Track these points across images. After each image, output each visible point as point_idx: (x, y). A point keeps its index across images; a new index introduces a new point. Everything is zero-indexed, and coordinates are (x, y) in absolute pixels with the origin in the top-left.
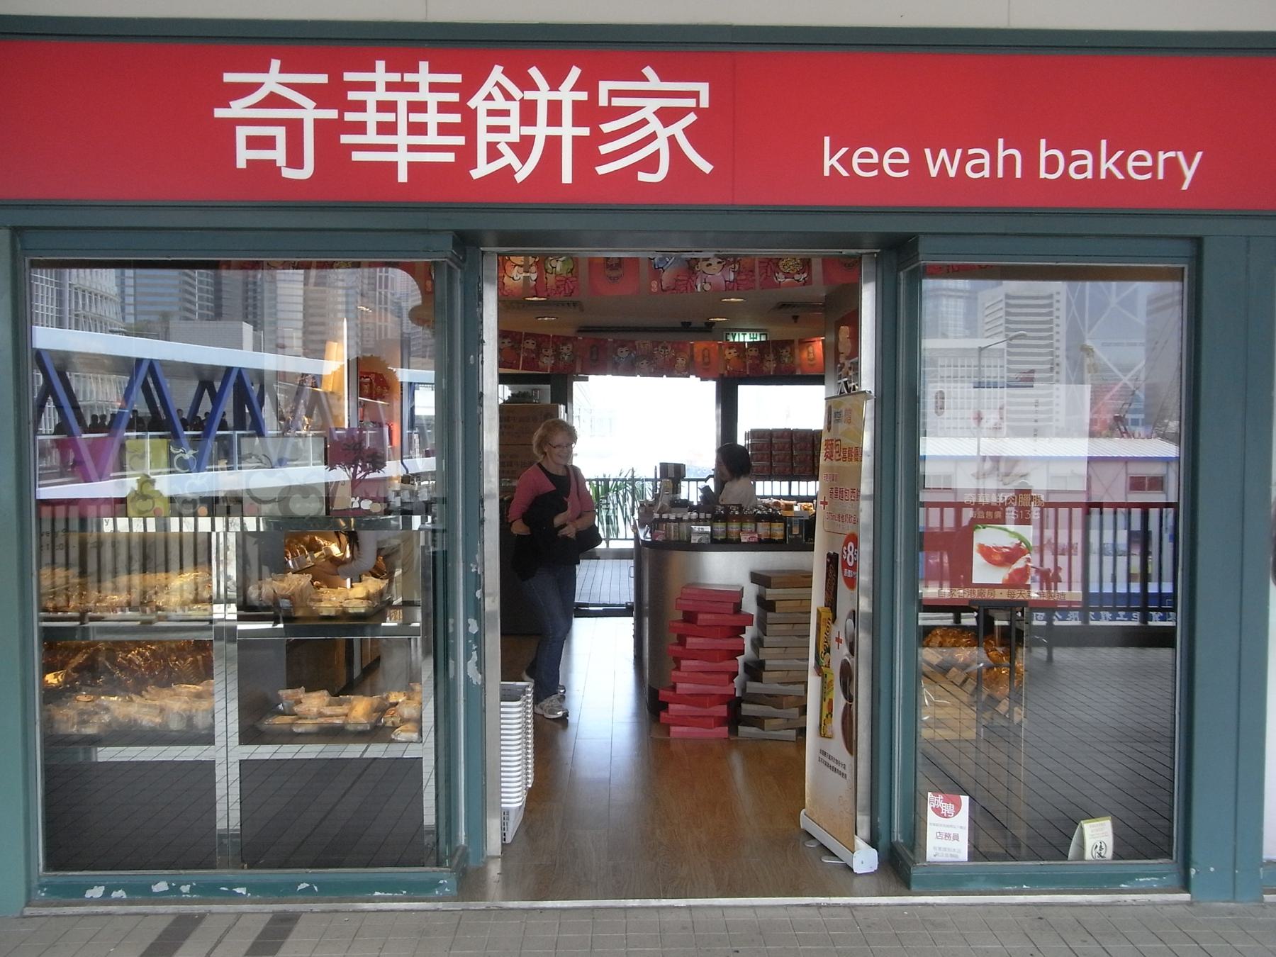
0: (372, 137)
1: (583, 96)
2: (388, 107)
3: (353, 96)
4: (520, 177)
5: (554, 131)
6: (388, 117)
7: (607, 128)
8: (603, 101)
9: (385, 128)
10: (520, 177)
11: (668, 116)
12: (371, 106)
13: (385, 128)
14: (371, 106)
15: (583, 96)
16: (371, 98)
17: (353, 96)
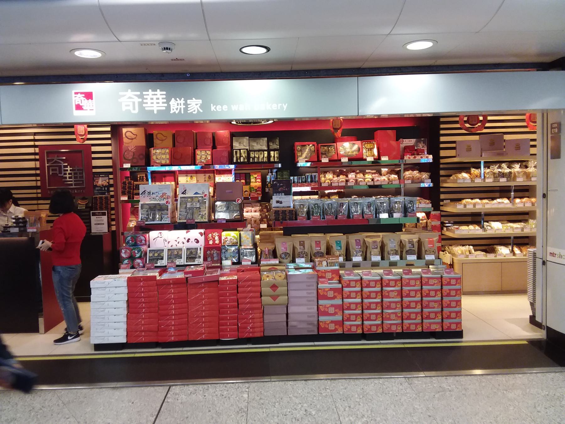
0: (149, 105)
1: (184, 102)
2: (152, 99)
3: (145, 97)
4: (177, 113)
5: (180, 107)
6: (152, 101)
7: (189, 106)
8: (188, 103)
9: (152, 103)
10: (177, 113)
11: (196, 105)
12: (149, 99)
13: (152, 103)
14: (149, 99)
15: (184, 102)
16: (149, 97)
17: (145, 97)
